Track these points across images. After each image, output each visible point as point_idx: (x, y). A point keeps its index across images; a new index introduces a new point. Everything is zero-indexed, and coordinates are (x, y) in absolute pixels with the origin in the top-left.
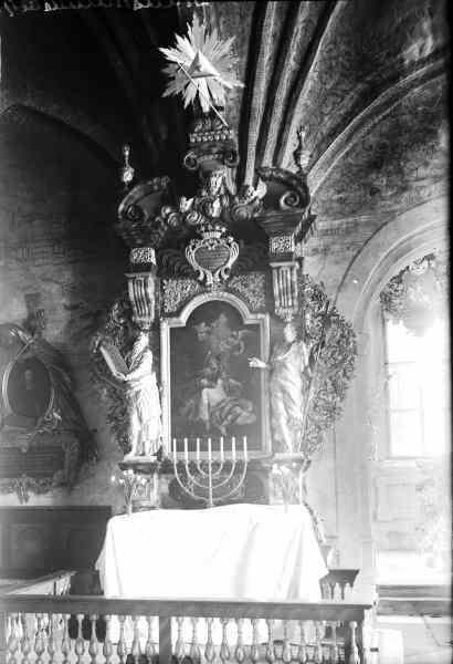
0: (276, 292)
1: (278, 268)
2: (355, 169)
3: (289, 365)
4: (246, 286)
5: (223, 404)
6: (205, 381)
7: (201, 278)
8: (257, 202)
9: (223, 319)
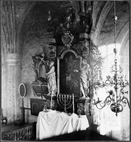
0: (82, 50)
1: (81, 43)
2: (119, 5)
3: (83, 72)
4: (76, 47)
5: (71, 81)
6: (67, 75)
7: (65, 46)
8: (78, 23)
9: (71, 57)
